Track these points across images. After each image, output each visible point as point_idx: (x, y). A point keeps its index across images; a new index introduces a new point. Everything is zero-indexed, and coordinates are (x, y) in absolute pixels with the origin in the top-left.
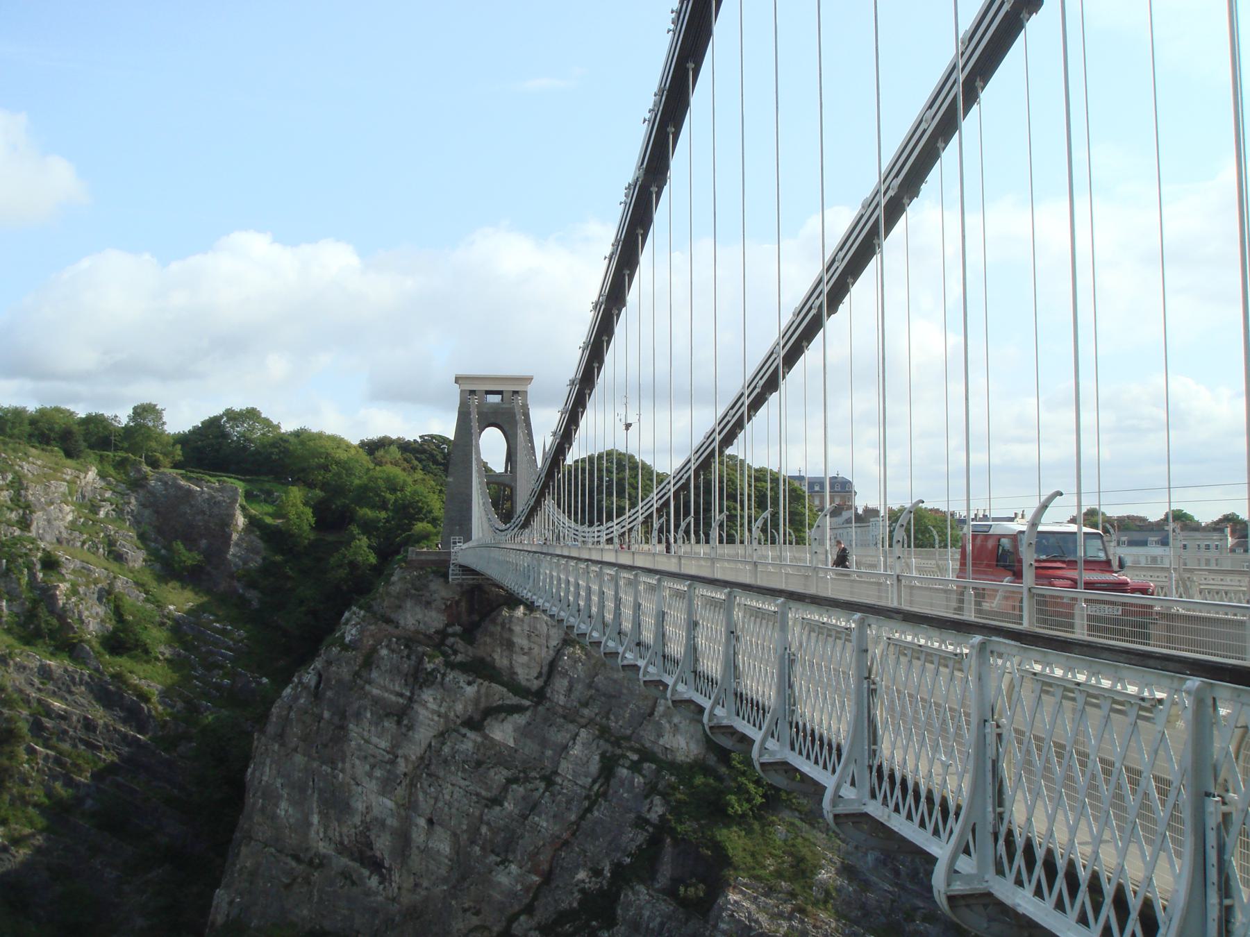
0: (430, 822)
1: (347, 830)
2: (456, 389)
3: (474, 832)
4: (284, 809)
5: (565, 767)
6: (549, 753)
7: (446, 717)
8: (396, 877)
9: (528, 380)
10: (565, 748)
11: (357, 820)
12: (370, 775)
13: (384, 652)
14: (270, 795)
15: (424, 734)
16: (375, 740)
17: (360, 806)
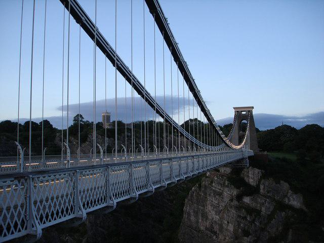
0: (228, 222)
1: (208, 224)
2: (234, 110)
3: (239, 225)
4: (192, 218)
5: (263, 209)
6: (259, 205)
7: (232, 195)
8: (220, 236)
9: (253, 108)
10: (263, 204)
11: (210, 221)
12: (213, 210)
13: (216, 178)
14: (189, 214)
15: (227, 200)
16: (214, 201)
17: (210, 217)
